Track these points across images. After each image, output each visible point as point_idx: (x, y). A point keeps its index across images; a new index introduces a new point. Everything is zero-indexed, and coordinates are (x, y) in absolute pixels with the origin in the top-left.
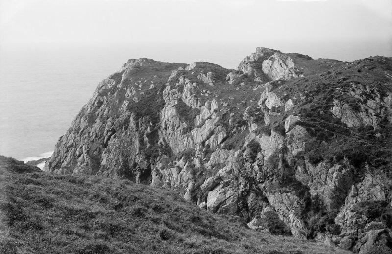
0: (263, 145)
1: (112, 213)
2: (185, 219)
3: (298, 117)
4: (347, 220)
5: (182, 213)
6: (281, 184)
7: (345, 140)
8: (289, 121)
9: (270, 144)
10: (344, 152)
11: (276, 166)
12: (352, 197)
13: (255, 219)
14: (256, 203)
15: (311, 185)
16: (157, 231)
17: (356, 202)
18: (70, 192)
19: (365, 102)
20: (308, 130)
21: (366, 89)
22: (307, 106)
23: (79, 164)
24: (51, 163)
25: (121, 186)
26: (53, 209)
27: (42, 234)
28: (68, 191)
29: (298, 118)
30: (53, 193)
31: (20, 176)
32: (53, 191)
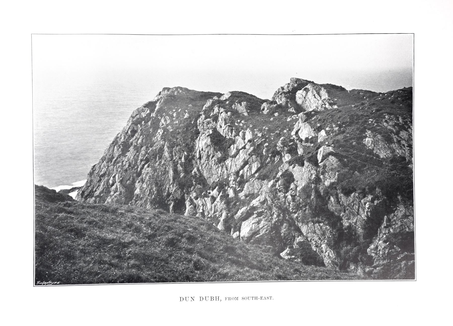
0: (296, 175)
1: (146, 242)
2: (219, 249)
3: (331, 148)
4: (380, 250)
5: (216, 243)
6: (313, 214)
7: (378, 171)
8: (322, 152)
9: (303, 175)
10: (376, 183)
11: (309, 196)
12: (385, 227)
13: (288, 249)
14: (289, 234)
15: (343, 216)
16: (190, 261)
17: (389, 233)
18: (103, 221)
19: (397, 133)
20: (340, 160)
21: (398, 120)
22: (340, 137)
23: (112, 193)
24: (83, 192)
25: (155, 215)
26: (85, 238)
27: (74, 264)
28: (100, 220)
29: (331, 149)
30: (85, 222)
31: (52, 206)
32: (85, 220)
